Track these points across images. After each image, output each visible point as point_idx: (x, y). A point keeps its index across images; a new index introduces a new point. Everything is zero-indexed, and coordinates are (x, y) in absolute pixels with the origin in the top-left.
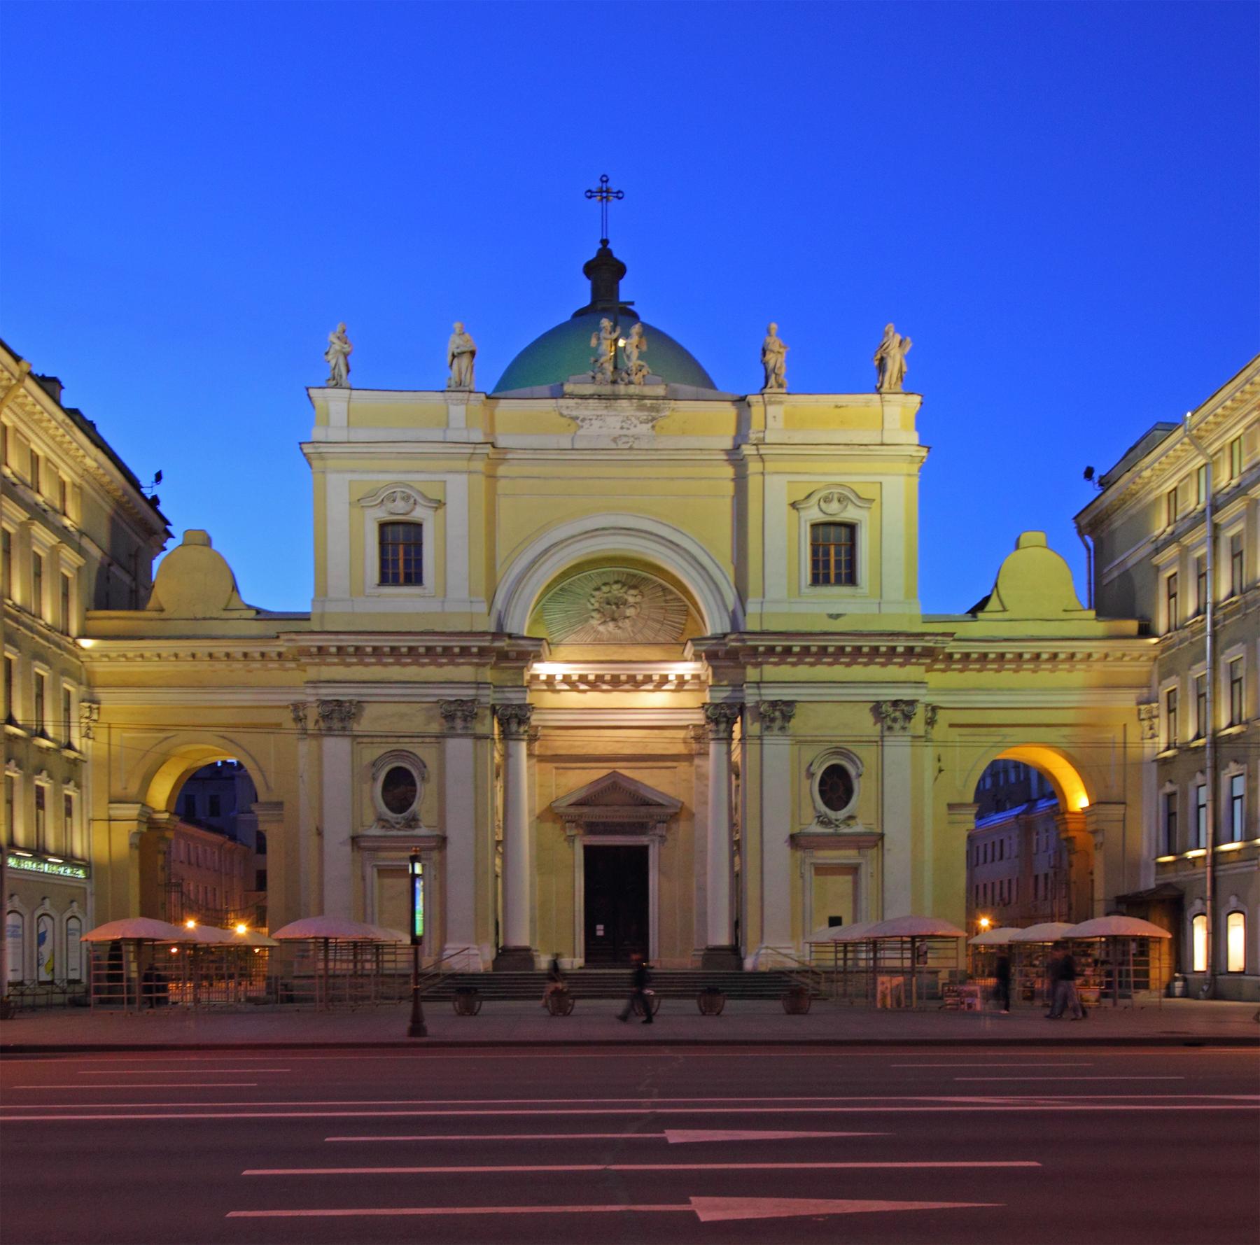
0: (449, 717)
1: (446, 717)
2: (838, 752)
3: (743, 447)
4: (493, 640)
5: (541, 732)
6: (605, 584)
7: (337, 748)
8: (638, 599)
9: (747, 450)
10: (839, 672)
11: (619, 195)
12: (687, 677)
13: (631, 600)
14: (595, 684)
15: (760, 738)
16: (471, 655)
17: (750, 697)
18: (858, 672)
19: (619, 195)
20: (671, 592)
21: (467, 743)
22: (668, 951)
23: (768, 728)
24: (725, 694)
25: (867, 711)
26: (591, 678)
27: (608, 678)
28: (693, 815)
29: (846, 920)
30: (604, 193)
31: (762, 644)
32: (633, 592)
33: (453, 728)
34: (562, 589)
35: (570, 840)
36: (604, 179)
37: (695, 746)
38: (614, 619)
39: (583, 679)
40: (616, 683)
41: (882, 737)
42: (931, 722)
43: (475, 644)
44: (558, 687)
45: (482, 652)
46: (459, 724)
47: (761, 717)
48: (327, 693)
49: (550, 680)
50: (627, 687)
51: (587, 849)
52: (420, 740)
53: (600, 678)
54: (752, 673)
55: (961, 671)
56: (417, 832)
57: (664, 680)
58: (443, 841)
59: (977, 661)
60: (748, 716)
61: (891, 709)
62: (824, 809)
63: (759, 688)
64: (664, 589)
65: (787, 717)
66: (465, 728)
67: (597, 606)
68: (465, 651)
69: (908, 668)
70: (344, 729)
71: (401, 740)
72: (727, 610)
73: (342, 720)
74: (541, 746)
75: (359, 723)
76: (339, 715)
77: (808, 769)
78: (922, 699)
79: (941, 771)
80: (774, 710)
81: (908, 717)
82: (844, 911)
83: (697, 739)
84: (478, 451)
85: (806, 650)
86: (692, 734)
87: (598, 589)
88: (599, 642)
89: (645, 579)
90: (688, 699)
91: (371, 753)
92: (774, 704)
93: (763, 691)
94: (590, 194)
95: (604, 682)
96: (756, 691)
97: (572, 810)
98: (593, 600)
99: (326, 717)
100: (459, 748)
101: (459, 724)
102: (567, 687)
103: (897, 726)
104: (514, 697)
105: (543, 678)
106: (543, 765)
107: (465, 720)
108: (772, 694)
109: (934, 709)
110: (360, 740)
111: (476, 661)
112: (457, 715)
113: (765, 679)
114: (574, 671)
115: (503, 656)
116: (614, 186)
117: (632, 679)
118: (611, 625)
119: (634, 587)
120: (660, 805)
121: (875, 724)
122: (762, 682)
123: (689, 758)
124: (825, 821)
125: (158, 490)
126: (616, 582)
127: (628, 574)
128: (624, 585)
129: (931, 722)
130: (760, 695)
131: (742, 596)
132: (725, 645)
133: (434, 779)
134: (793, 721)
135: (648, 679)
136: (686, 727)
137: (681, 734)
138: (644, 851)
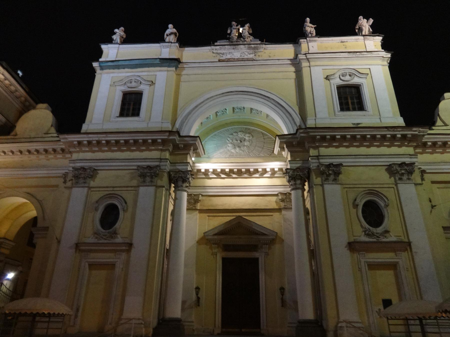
0: (143, 176)
1: (140, 176)
2: (371, 192)
3: (299, 55)
4: (169, 136)
5: (201, 198)
6: (235, 132)
7: (79, 194)
9: (301, 57)
10: (363, 150)
12: (276, 170)
13: (247, 138)
14: (229, 174)
15: (322, 185)
16: (159, 144)
17: (313, 164)
18: (373, 150)
20: (267, 135)
23: (327, 179)
24: (298, 165)
25: (384, 171)
26: (227, 170)
27: (235, 170)
28: (283, 240)
29: (395, 300)
31: (318, 134)
33: (144, 182)
34: (215, 135)
37: (282, 205)
38: (239, 147)
39: (223, 171)
40: (239, 173)
41: (396, 184)
42: (423, 179)
43: (159, 137)
44: (210, 176)
45: (164, 142)
46: (148, 179)
47: (321, 173)
48: (79, 165)
49: (206, 172)
50: (246, 176)
51: (224, 259)
52: (125, 189)
53: (231, 171)
54: (313, 152)
55: (431, 153)
57: (265, 171)
58: (130, 245)
59: (440, 147)
60: (313, 176)
61: (399, 169)
62: (367, 226)
63: (318, 159)
64: (263, 134)
65: (337, 174)
66: (152, 181)
68: (154, 142)
69: (404, 148)
70: (85, 183)
71: (115, 189)
72: (296, 125)
73: (85, 178)
74: (201, 205)
75: (94, 181)
77: (354, 203)
79: (433, 207)
80: (329, 170)
81: (411, 173)
82: (391, 293)
83: (282, 200)
85: (344, 138)
86: (280, 197)
87: (232, 134)
88: (232, 156)
89: (254, 130)
90: (276, 181)
91: (96, 196)
92: (329, 166)
93: (321, 161)
95: (234, 173)
96: (317, 161)
97: (216, 237)
99: (76, 177)
100: (146, 192)
101: (148, 179)
102: (215, 176)
103: (405, 177)
104: (180, 167)
105: (203, 171)
106: (202, 214)
107: (152, 177)
109: (423, 172)
110: (92, 189)
111: (161, 148)
112: (148, 174)
113: (321, 154)
114: (219, 167)
115: (176, 147)
117: (248, 171)
118: (238, 149)
119: (249, 133)
120: (264, 234)
121: (390, 178)
122: (319, 156)
123: (279, 210)
124: (368, 235)
126: (240, 131)
127: (246, 129)
129: (423, 179)
130: (319, 162)
131: (304, 118)
132: (297, 138)
133: (130, 210)
134: (341, 176)
135: (256, 171)
136: (277, 195)
137: (274, 198)
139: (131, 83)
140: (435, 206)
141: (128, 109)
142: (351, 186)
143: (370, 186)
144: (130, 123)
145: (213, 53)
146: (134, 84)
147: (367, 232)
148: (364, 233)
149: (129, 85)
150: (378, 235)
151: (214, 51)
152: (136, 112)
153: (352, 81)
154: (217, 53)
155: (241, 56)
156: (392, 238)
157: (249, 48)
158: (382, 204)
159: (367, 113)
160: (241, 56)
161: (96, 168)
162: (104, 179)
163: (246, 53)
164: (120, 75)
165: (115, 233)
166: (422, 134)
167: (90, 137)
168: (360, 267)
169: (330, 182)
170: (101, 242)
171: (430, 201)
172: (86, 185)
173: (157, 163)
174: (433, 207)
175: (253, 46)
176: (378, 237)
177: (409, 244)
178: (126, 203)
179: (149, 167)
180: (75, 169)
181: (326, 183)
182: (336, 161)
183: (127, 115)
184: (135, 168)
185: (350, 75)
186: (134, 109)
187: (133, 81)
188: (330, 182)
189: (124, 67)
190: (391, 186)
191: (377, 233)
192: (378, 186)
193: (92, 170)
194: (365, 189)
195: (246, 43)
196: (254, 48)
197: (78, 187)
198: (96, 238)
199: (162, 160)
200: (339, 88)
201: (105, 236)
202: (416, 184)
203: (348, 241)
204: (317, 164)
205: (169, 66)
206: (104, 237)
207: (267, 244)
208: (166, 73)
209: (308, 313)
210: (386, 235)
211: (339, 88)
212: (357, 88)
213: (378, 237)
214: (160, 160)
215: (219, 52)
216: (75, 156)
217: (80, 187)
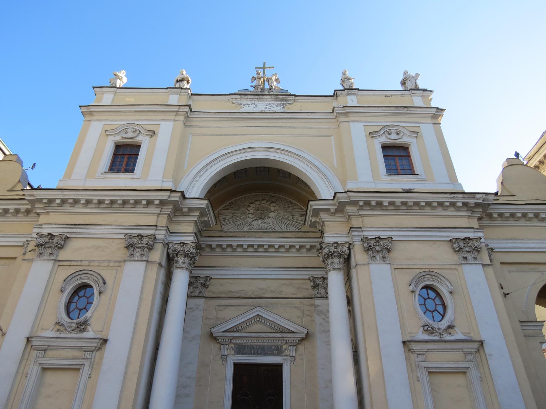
1: (127, 247)
8: (277, 207)
21: (141, 266)
32: (274, 204)
34: (231, 203)
35: (224, 357)
38: (261, 218)
43: (157, 197)
52: (106, 264)
56: (85, 335)
58: (105, 341)
62: (427, 319)
67: (251, 211)
71: (92, 264)
76: (51, 245)
84: (180, 110)
87: (252, 203)
96: (361, 234)
98: (249, 209)
110: (61, 263)
112: (137, 246)
118: (260, 221)
128: (268, 201)
138: (279, 368)
139: (127, 132)
140: (508, 294)
141: (121, 164)
142: (404, 267)
143: (427, 267)
144: (121, 180)
145: (233, 103)
146: (130, 135)
147: (426, 328)
148: (422, 329)
150: (440, 331)
151: (234, 102)
152: (130, 168)
153: (399, 140)
154: (238, 104)
155: (266, 108)
156: (459, 336)
157: (276, 100)
159: (419, 177)
160: (266, 108)
161: (69, 236)
163: (272, 105)
164: (114, 123)
166: (487, 202)
167: (65, 195)
168: (419, 375)
169: (377, 262)
170: (62, 335)
171: (502, 288)
172: (53, 257)
173: (152, 232)
174: (505, 295)
175: (281, 97)
176: (440, 334)
177: (481, 343)
178: (105, 283)
179: (141, 237)
180: (40, 235)
181: (371, 261)
182: (383, 234)
183: (119, 171)
184: (123, 237)
185: (398, 133)
186: (127, 164)
187: (130, 130)
188: (377, 262)
190: (453, 267)
191: (439, 329)
192: (437, 267)
193: (63, 237)
194: (420, 271)
195: (272, 93)
196: (283, 100)
197: (40, 259)
198: (58, 330)
199: (159, 228)
200: (385, 147)
201: (71, 327)
202: (484, 266)
203: (401, 340)
204: (360, 238)
206: (69, 330)
207: (294, 346)
208: (172, 123)
210: (451, 331)
211: (385, 147)
213: (440, 334)
214: (155, 228)
215: (239, 102)
216: (43, 219)
217: (44, 260)
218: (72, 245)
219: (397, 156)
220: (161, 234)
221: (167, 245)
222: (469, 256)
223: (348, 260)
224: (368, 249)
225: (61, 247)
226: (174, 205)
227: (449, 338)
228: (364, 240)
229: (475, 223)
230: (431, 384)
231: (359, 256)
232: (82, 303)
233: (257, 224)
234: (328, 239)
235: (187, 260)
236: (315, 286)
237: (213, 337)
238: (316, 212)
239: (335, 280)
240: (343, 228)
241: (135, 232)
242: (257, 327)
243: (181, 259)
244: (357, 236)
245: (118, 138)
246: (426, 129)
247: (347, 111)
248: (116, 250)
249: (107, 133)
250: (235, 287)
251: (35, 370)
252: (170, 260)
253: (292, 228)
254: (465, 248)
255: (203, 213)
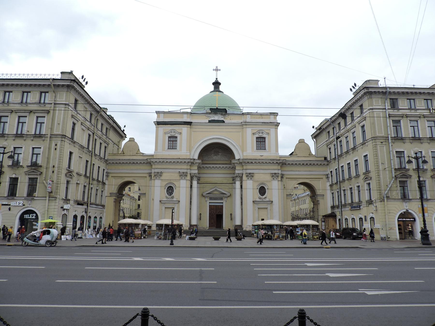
2: (263, 184)
7: (157, 183)
11: (220, 70)
17: (244, 172)
19: (220, 70)
21: (185, 181)
22: (227, 224)
30: (217, 70)
35: (206, 201)
36: (217, 67)
42: (282, 177)
43: (187, 161)
76: (159, 175)
78: (280, 173)
94: (214, 70)
101: (183, 178)
108: (249, 171)
112: (183, 175)
116: (219, 68)
125: (124, 129)
129: (282, 177)
149: (171, 134)
156: (267, 200)
158: (266, 188)
162: (166, 176)
165: (173, 197)
177: (272, 202)
189: (168, 124)
205: (187, 125)
209: (238, 223)
212: (265, 138)
218: (164, 174)
219: (261, 142)
220: (189, 171)
221: (190, 174)
222: (275, 178)
223: (241, 178)
224: (247, 176)
225: (161, 176)
226: (192, 163)
227: (264, 200)
228: (246, 173)
229: (279, 167)
230: (258, 211)
231: (244, 177)
232: (170, 191)
233: (215, 157)
234: (237, 172)
235: (196, 178)
236: (233, 180)
237: (203, 196)
238: (234, 163)
239: (238, 184)
240: (241, 168)
241: (182, 171)
242: (216, 192)
243: (195, 178)
244: (244, 172)
245: (169, 135)
246: (272, 131)
247: (245, 124)
248: (177, 176)
249: (165, 133)
250: (209, 180)
251: (164, 208)
252: (192, 178)
253: (226, 159)
254: (274, 176)
255: (199, 163)
